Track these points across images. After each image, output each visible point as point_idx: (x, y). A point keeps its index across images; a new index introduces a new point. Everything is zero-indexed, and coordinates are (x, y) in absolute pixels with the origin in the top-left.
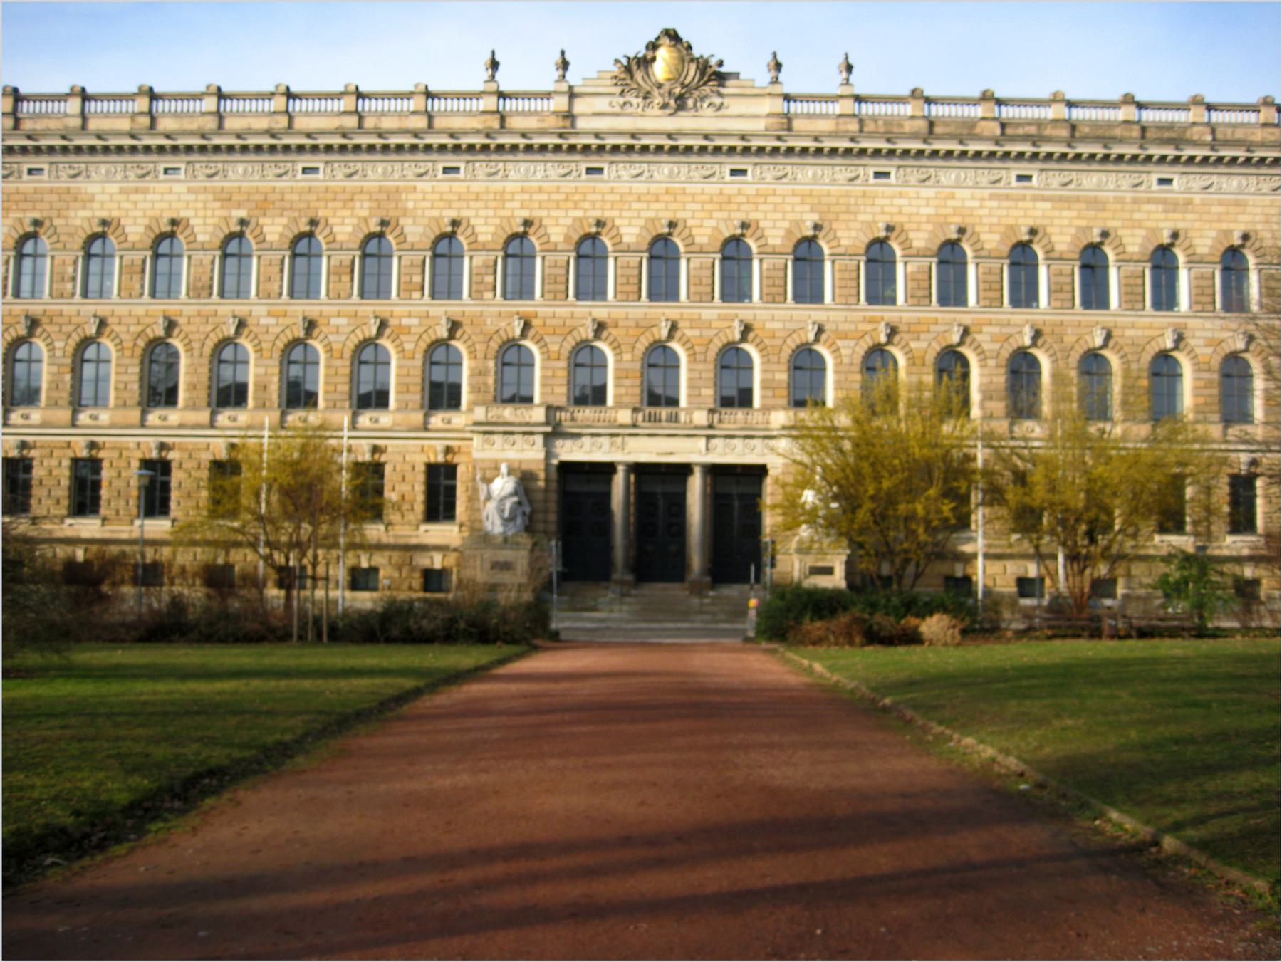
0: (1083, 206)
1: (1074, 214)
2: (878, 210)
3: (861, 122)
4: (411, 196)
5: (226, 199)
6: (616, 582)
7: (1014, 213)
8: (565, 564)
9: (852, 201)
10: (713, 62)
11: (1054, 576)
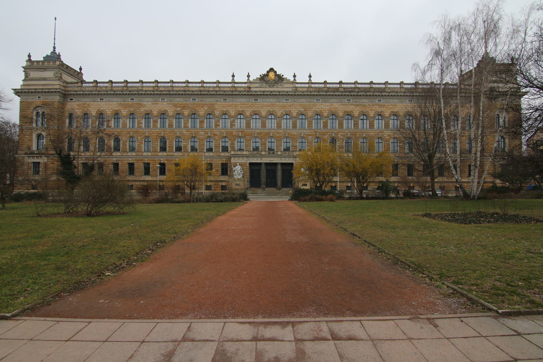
0: (361, 106)
1: (359, 108)
2: (317, 108)
4: (216, 105)
5: (175, 106)
6: (262, 188)
7: (346, 108)
8: (250, 185)
9: (311, 106)
10: (281, 75)
11: (354, 185)
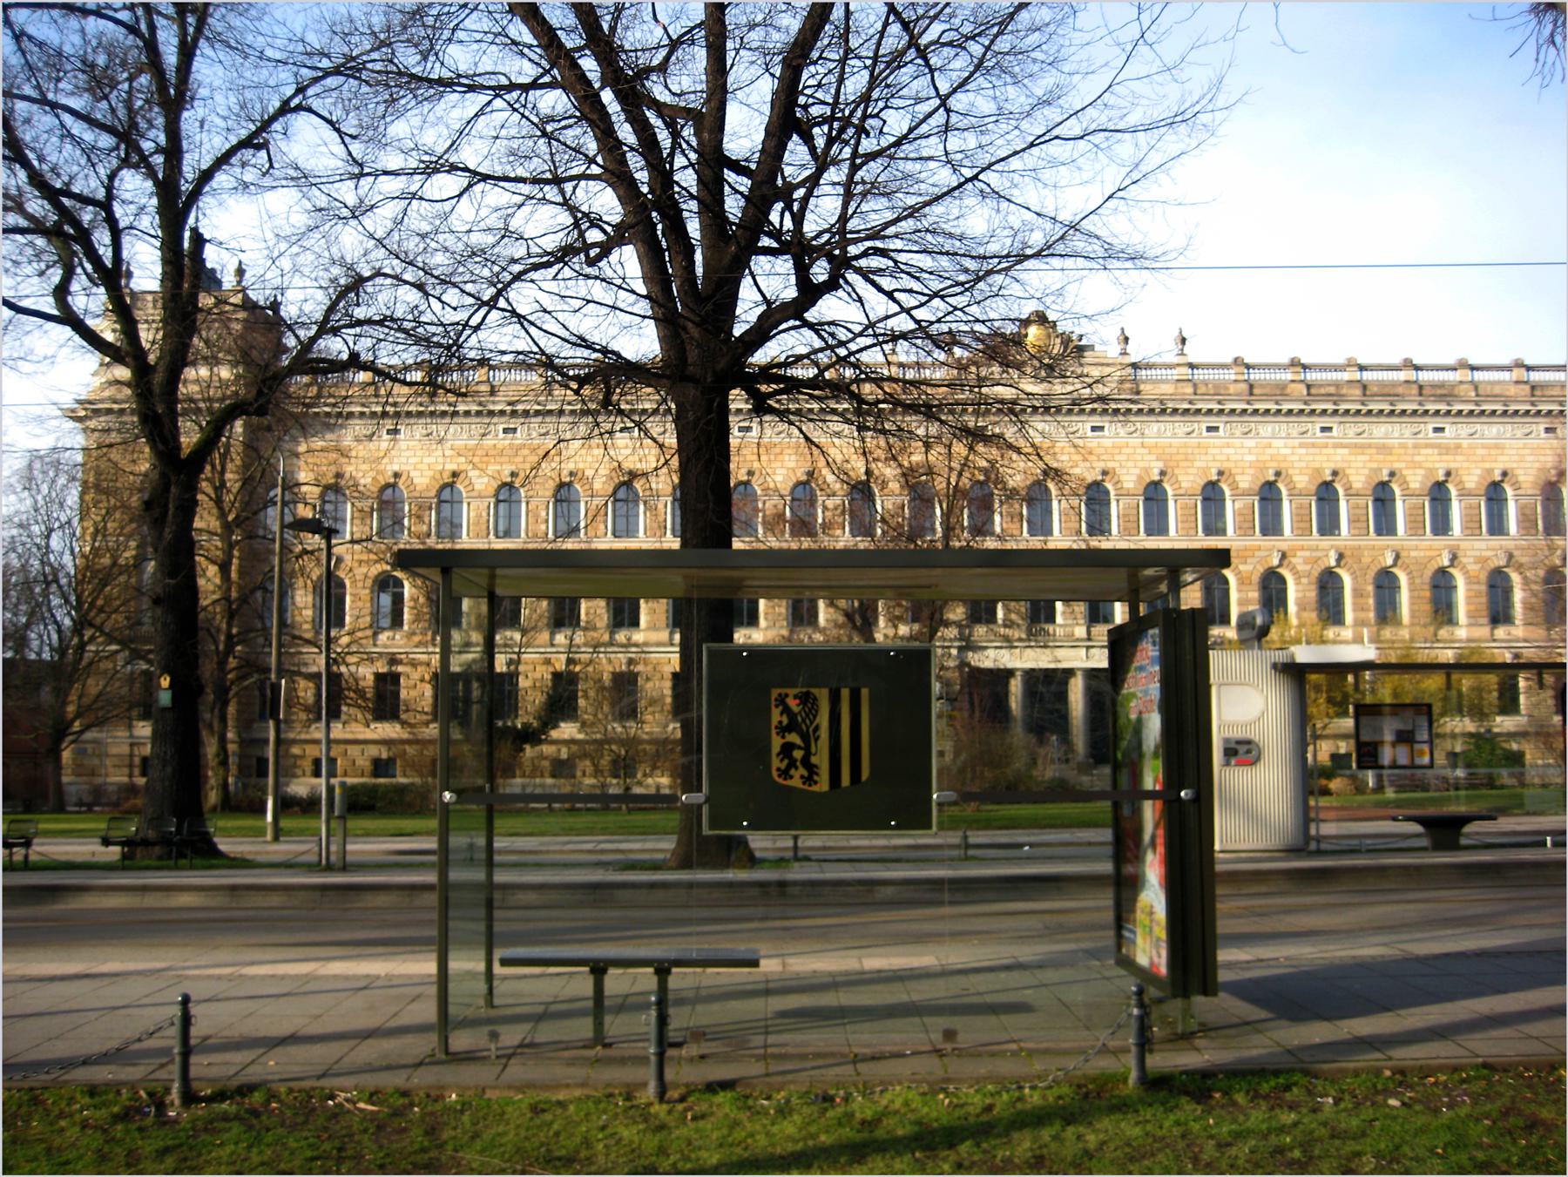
3: (1195, 386)
7: (1318, 458)
